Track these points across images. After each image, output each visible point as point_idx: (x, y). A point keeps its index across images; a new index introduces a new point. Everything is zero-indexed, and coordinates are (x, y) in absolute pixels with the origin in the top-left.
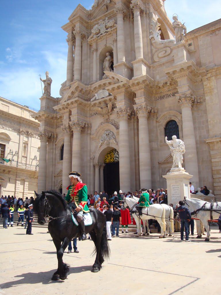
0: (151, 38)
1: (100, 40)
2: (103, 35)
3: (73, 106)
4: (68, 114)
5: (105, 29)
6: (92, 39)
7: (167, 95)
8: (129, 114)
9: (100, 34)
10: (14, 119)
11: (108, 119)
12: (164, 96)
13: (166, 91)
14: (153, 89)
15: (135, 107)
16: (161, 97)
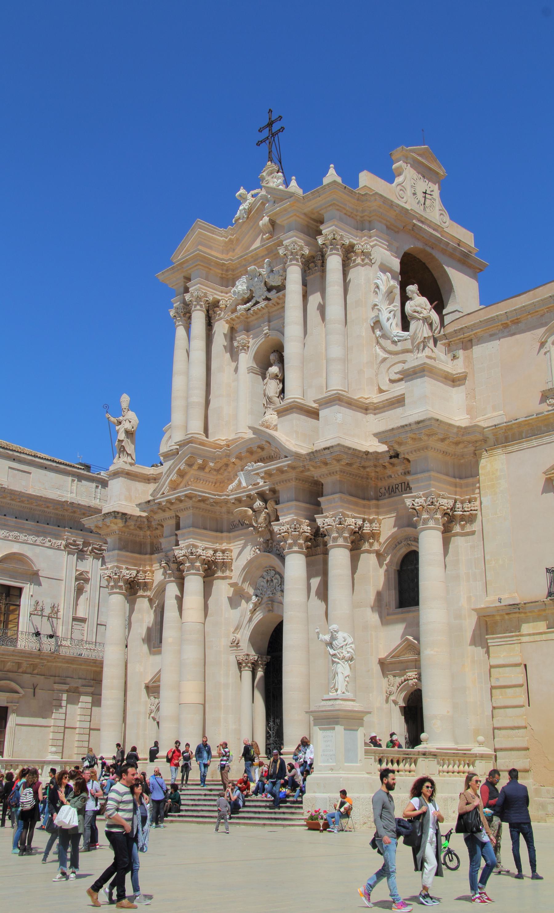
0: (374, 324)
1: (254, 318)
2: (258, 306)
3: (182, 506)
4: (173, 522)
5: (265, 289)
6: (233, 316)
7: (403, 484)
8: (307, 537)
9: (253, 301)
10: (46, 509)
11: (270, 541)
12: (397, 486)
13: (400, 474)
14: (368, 470)
15: (319, 522)
16: (391, 488)
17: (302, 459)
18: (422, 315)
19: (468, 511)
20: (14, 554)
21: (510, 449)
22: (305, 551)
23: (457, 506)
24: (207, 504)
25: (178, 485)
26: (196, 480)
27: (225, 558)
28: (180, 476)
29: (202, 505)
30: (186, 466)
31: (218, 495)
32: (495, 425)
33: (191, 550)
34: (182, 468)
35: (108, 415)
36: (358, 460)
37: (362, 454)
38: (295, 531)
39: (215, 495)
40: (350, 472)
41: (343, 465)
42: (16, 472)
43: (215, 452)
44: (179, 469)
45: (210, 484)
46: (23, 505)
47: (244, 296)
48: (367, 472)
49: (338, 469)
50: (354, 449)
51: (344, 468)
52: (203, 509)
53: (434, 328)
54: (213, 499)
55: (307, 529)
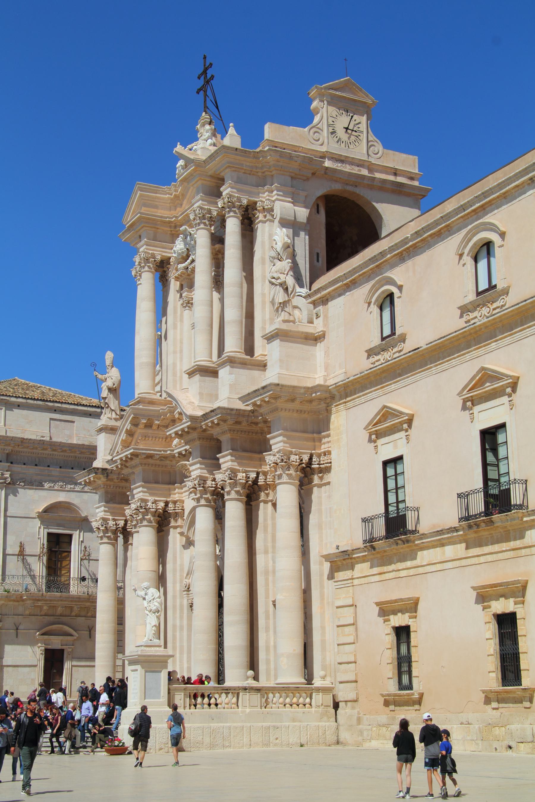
14: (260, 425)
17: (198, 421)
18: (279, 281)
19: (324, 464)
20: (60, 503)
21: (349, 404)
22: (212, 505)
23: (314, 460)
24: (156, 460)
25: (130, 443)
26: (143, 438)
27: (176, 508)
28: (130, 435)
29: (150, 461)
30: (132, 426)
31: (164, 451)
32: (336, 384)
33: (140, 504)
34: (128, 428)
35: (96, 373)
36: (245, 419)
37: (248, 413)
38: (200, 487)
39: (161, 451)
40: (242, 430)
41: (231, 425)
42: (59, 422)
43: (159, 410)
44: (127, 429)
45: (160, 440)
46: (66, 454)
47: (182, 254)
48: (260, 427)
49: (227, 429)
50: (237, 410)
51: (232, 427)
52: (152, 465)
53: (289, 293)
54: (159, 455)
55: (212, 484)
